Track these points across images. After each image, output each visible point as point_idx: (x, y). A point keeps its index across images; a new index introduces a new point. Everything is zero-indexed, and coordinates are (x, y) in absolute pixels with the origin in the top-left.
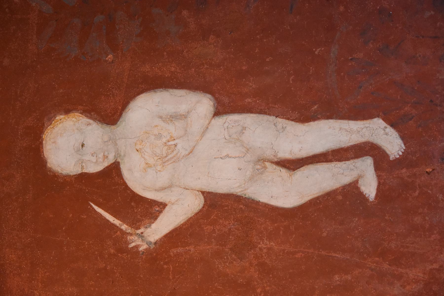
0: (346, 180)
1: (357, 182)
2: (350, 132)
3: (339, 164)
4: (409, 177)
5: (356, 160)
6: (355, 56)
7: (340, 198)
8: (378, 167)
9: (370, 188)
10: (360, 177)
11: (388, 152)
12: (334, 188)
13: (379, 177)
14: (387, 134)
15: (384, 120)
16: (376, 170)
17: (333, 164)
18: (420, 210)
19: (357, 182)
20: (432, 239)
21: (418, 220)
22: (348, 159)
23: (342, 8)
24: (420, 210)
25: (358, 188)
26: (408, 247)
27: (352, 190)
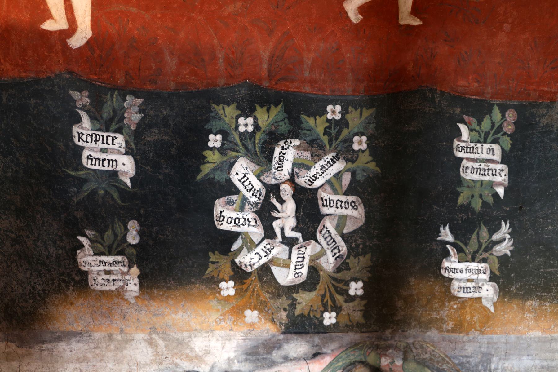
0: (53, 12)
1: (52, 18)
2: (84, 17)
3: (63, 8)
4: (56, 50)
5: (66, 19)
6: (130, 22)
7: (42, 7)
8: (61, 32)
9: (48, 26)
10: (56, 21)
11: (71, 39)
12: (48, 4)
13: (55, 32)
14: (82, 38)
15: (91, 37)
16: (60, 30)
17: (63, 4)
18: (36, 55)
19: (52, 18)
20: (19, 60)
21: (30, 53)
22: (66, 14)
23: (159, 16)
24: (36, 55)
25: (48, 19)
26: (13, 46)
27: (47, 15)
